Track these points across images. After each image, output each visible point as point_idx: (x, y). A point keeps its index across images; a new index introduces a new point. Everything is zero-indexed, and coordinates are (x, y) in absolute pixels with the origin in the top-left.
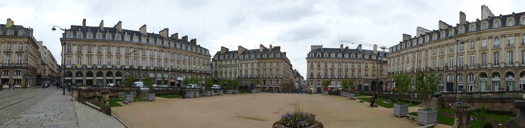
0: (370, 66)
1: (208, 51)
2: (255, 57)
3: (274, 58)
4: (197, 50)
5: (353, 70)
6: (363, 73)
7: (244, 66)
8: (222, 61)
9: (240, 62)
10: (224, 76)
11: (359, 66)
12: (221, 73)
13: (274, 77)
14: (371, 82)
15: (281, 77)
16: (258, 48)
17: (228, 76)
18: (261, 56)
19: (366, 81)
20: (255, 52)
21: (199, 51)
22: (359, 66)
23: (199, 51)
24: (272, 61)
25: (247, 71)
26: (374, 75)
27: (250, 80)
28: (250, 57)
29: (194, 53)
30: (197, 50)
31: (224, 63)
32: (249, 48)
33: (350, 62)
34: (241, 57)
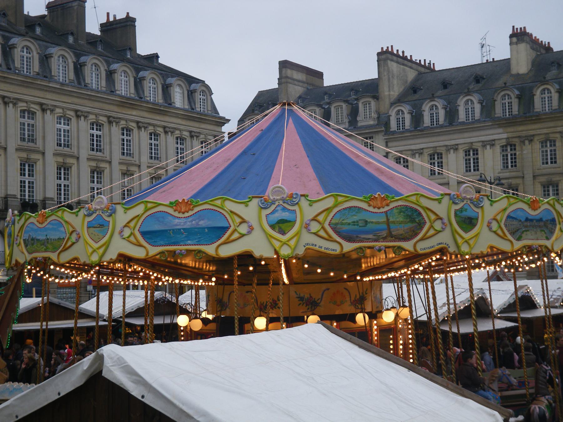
1: (208, 91)
2: (488, 108)
4: (139, 83)
16: (501, 50)
18: (526, 98)
20: (481, 79)
21: (152, 91)
23: (152, 91)
28: (451, 114)
29: (126, 103)
30: (139, 83)
32: (443, 62)
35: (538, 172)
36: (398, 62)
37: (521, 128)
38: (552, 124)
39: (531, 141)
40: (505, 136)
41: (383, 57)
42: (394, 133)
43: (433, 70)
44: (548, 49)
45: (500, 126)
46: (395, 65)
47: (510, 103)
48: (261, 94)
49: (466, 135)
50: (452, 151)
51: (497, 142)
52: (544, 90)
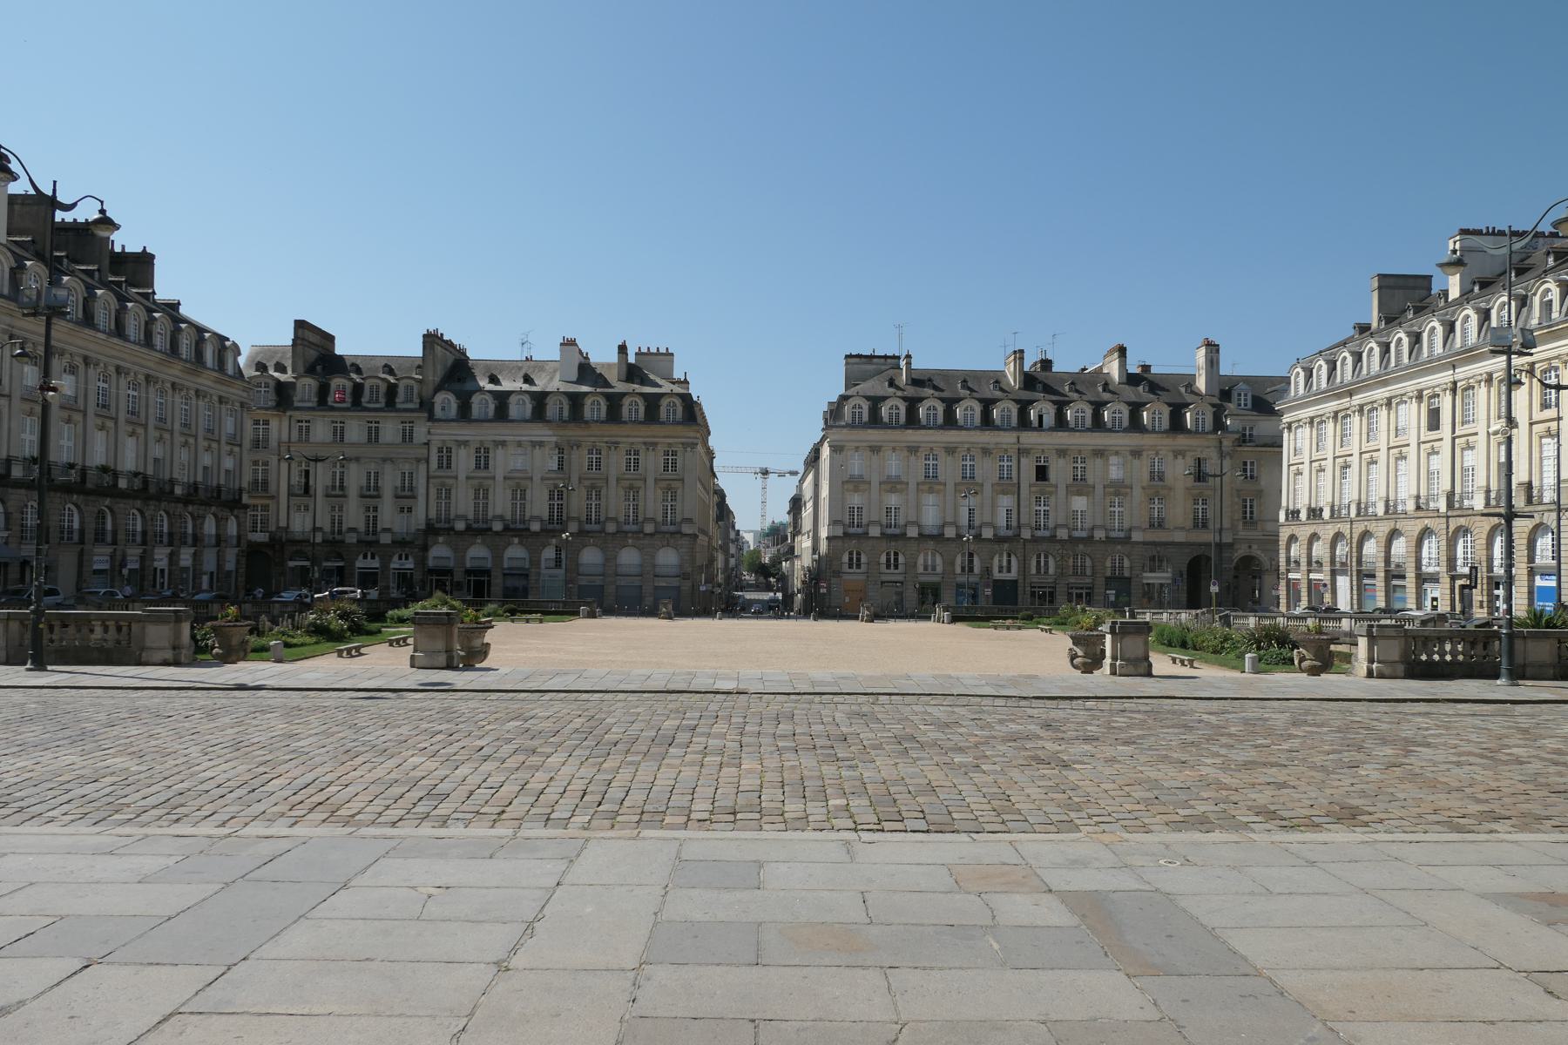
7: (464, 461)
13: (649, 528)
15: (686, 529)
16: (548, 351)
25: (482, 493)
26: (1201, 524)
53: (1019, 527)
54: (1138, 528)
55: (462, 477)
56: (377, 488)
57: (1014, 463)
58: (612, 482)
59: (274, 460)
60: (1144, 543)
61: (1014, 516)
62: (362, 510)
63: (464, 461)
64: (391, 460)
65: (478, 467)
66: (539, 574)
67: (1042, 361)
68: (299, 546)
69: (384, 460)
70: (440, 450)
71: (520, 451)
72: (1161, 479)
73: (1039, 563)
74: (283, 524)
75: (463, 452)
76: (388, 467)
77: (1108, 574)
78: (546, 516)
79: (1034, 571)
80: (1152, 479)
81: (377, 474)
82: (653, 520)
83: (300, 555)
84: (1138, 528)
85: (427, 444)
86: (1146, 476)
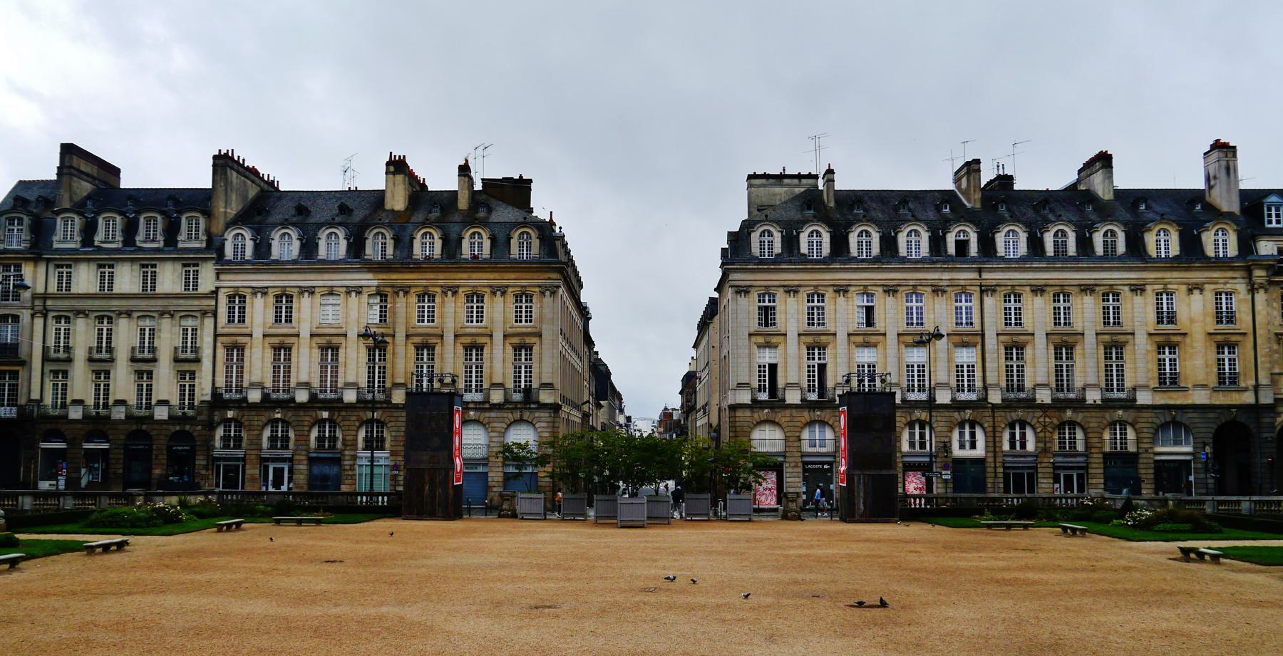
0: (1195, 310)
2: (356, 248)
3: (499, 261)
5: (1064, 345)
6: (1140, 367)
7: (260, 313)
8: (66, 261)
9: (233, 281)
10: (81, 384)
11: (1111, 317)
12: (58, 364)
13: (497, 397)
14: (1206, 429)
15: (546, 397)
16: (373, 179)
17: (123, 384)
19: (1173, 420)
22: (1111, 317)
24: (481, 280)
26: (1227, 380)
27: (307, 419)
31: (85, 279)
32: (291, 177)
33: (1038, 290)
34: (239, 242)
35: (412, 331)
36: (238, 172)
37: (394, 276)
38: (431, 276)
39: (406, 293)
40: (375, 283)
41: (221, 162)
42: (229, 262)
43: (277, 189)
44: (424, 186)
45: (370, 270)
46: (235, 174)
47: (384, 244)
48: (22, 185)
49: (326, 276)
50: (306, 294)
51: (365, 290)
52: (425, 234)
53: (985, 388)
54: (1145, 387)
55: (258, 333)
56: (153, 349)
57: (975, 303)
58: (449, 337)
59: (25, 316)
60: (1153, 407)
61: (978, 374)
62: (133, 377)
63: (260, 313)
64: (169, 312)
65: (278, 319)
66: (355, 458)
67: (999, 177)
68: (56, 425)
69: (162, 314)
70: (231, 298)
71: (332, 300)
72: (1172, 319)
73: (1013, 436)
74: (35, 395)
75: (259, 301)
76: (166, 323)
77: (1107, 449)
78: (363, 383)
79: (1006, 447)
80: (1160, 320)
81: (152, 331)
82: (501, 385)
83: (58, 436)
84: (1145, 387)
85: (215, 293)
86: (1152, 316)
